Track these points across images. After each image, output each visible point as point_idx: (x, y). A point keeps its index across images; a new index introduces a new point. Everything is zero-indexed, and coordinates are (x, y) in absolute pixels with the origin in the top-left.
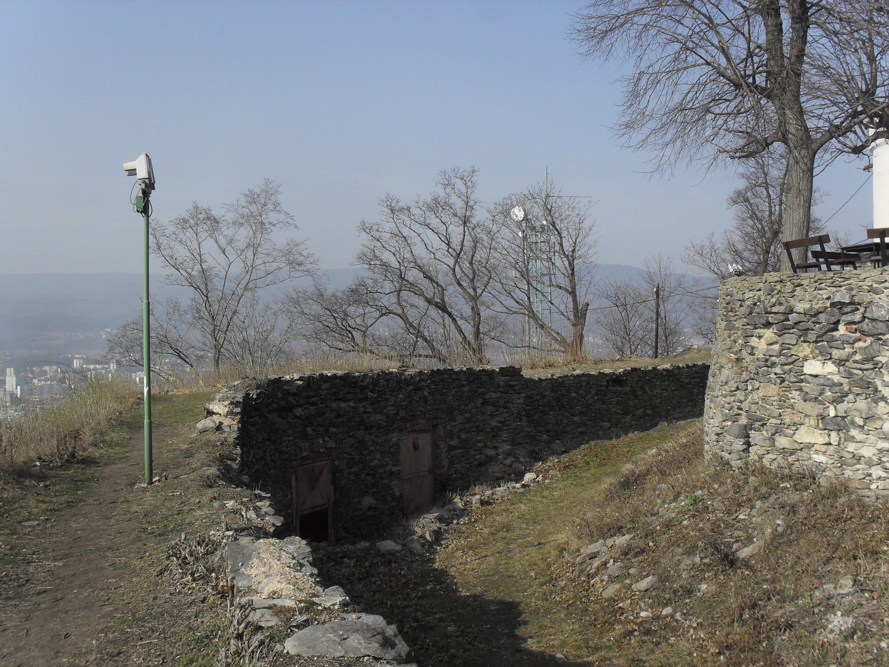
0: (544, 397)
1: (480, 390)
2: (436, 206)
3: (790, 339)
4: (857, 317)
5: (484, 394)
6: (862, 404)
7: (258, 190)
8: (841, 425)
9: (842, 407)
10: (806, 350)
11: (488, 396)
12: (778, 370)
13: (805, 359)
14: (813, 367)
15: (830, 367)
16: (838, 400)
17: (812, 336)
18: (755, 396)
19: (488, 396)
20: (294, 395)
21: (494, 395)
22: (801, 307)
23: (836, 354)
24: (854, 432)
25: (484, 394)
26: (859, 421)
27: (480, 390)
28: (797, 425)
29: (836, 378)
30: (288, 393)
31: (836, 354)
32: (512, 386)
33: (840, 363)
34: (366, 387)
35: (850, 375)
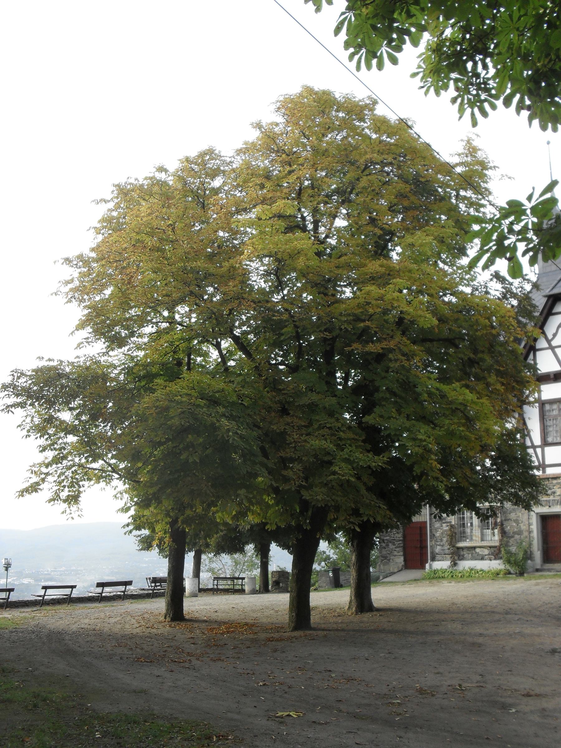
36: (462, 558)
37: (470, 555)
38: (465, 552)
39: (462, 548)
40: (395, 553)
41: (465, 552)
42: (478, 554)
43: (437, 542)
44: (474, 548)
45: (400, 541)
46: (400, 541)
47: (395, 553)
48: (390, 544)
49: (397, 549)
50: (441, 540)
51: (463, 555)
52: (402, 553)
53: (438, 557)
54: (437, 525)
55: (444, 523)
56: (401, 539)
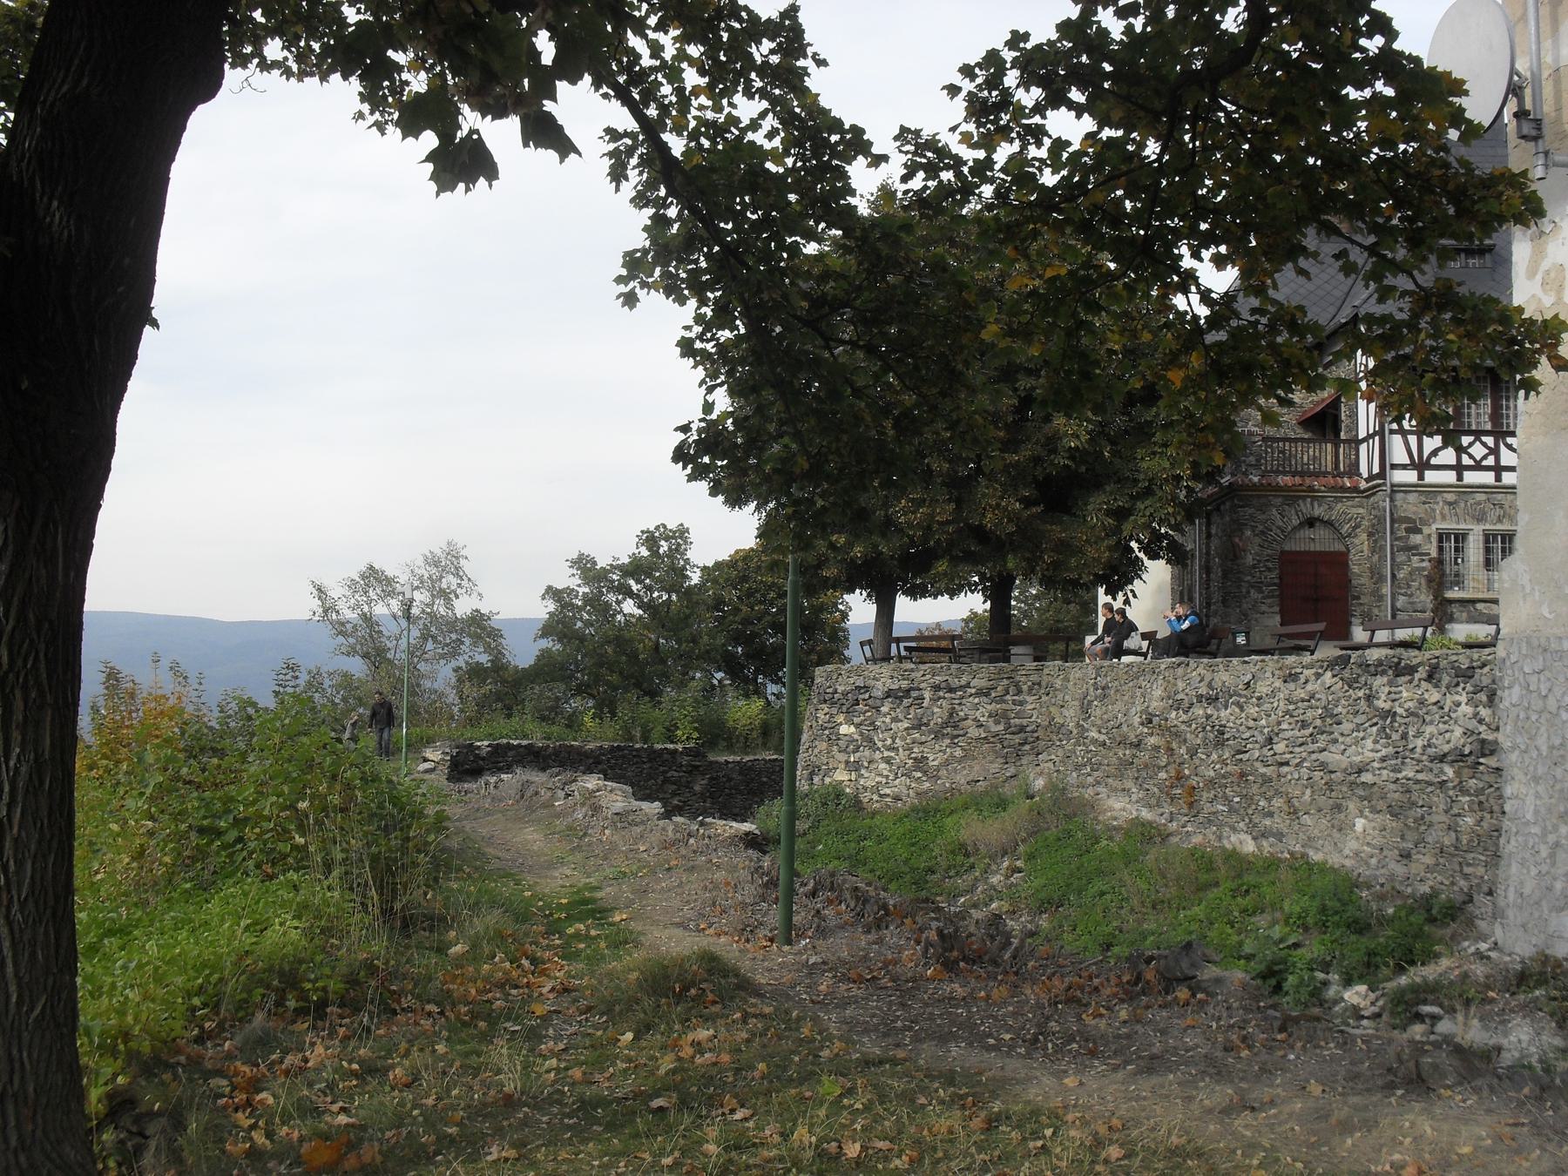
0: (730, 780)
1: (661, 769)
2: (636, 569)
3: (834, 711)
4: (867, 696)
5: (664, 772)
6: (867, 753)
7: (438, 552)
8: (855, 767)
9: (857, 755)
10: (841, 718)
11: (669, 775)
12: (827, 732)
13: (841, 724)
14: (844, 729)
15: (852, 729)
16: (856, 750)
17: (844, 709)
18: (816, 751)
19: (669, 775)
20: (483, 759)
21: (676, 774)
22: (840, 689)
23: (856, 720)
24: (863, 771)
25: (664, 772)
26: (866, 764)
27: (661, 769)
28: (836, 769)
29: (856, 737)
30: (477, 756)
31: (856, 720)
32: (697, 767)
33: (857, 726)
34: (550, 756)
35: (861, 734)
36: (1451, 619)
37: (1465, 615)
38: (1455, 609)
39: (1451, 601)
40: (1264, 608)
41: (1455, 609)
42: (1481, 614)
43: (1400, 588)
44: (1473, 602)
45: (1275, 584)
46: (1275, 584)
47: (1264, 608)
48: (1252, 591)
49: (1269, 601)
50: (1409, 587)
51: (1452, 614)
52: (1277, 609)
53: (1401, 616)
54: (1401, 557)
55: (1414, 555)
56: (1276, 581)
